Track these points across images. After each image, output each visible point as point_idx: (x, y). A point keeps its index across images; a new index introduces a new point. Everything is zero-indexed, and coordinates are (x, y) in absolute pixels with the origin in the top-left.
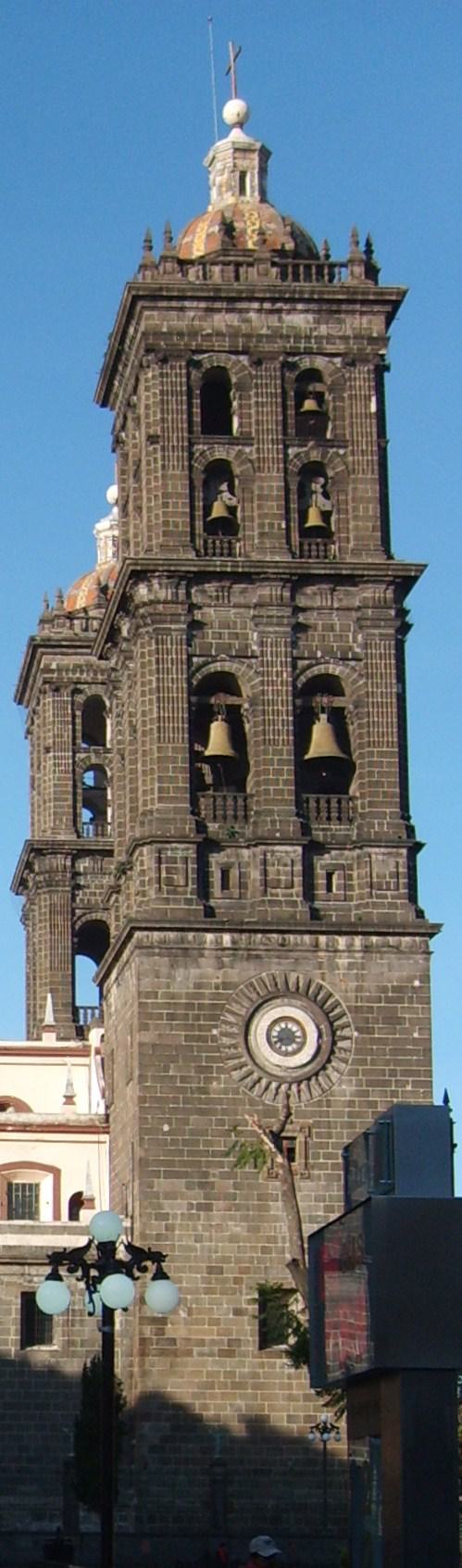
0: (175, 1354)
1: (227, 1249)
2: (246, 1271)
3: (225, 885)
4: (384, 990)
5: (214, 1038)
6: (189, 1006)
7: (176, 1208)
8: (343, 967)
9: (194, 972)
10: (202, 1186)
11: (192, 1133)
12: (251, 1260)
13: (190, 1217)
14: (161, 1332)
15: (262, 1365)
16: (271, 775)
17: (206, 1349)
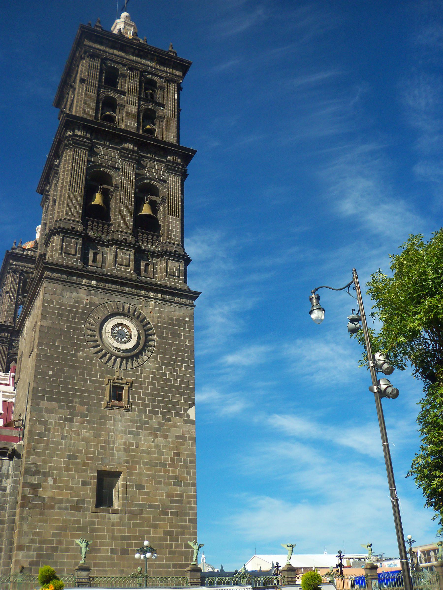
0: (44, 507)
1: (82, 446)
2: (91, 459)
3: (94, 260)
4: (172, 319)
5: (83, 329)
6: (70, 311)
7: (52, 419)
8: (152, 308)
9: (74, 295)
10: (68, 407)
11: (65, 377)
12: (94, 453)
13: (60, 425)
14: (35, 493)
15: (97, 517)
16: (121, 216)
17: (63, 505)
